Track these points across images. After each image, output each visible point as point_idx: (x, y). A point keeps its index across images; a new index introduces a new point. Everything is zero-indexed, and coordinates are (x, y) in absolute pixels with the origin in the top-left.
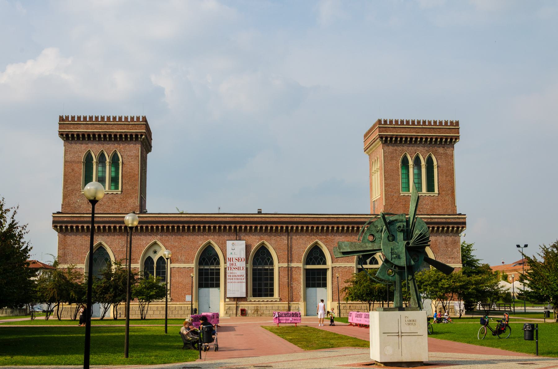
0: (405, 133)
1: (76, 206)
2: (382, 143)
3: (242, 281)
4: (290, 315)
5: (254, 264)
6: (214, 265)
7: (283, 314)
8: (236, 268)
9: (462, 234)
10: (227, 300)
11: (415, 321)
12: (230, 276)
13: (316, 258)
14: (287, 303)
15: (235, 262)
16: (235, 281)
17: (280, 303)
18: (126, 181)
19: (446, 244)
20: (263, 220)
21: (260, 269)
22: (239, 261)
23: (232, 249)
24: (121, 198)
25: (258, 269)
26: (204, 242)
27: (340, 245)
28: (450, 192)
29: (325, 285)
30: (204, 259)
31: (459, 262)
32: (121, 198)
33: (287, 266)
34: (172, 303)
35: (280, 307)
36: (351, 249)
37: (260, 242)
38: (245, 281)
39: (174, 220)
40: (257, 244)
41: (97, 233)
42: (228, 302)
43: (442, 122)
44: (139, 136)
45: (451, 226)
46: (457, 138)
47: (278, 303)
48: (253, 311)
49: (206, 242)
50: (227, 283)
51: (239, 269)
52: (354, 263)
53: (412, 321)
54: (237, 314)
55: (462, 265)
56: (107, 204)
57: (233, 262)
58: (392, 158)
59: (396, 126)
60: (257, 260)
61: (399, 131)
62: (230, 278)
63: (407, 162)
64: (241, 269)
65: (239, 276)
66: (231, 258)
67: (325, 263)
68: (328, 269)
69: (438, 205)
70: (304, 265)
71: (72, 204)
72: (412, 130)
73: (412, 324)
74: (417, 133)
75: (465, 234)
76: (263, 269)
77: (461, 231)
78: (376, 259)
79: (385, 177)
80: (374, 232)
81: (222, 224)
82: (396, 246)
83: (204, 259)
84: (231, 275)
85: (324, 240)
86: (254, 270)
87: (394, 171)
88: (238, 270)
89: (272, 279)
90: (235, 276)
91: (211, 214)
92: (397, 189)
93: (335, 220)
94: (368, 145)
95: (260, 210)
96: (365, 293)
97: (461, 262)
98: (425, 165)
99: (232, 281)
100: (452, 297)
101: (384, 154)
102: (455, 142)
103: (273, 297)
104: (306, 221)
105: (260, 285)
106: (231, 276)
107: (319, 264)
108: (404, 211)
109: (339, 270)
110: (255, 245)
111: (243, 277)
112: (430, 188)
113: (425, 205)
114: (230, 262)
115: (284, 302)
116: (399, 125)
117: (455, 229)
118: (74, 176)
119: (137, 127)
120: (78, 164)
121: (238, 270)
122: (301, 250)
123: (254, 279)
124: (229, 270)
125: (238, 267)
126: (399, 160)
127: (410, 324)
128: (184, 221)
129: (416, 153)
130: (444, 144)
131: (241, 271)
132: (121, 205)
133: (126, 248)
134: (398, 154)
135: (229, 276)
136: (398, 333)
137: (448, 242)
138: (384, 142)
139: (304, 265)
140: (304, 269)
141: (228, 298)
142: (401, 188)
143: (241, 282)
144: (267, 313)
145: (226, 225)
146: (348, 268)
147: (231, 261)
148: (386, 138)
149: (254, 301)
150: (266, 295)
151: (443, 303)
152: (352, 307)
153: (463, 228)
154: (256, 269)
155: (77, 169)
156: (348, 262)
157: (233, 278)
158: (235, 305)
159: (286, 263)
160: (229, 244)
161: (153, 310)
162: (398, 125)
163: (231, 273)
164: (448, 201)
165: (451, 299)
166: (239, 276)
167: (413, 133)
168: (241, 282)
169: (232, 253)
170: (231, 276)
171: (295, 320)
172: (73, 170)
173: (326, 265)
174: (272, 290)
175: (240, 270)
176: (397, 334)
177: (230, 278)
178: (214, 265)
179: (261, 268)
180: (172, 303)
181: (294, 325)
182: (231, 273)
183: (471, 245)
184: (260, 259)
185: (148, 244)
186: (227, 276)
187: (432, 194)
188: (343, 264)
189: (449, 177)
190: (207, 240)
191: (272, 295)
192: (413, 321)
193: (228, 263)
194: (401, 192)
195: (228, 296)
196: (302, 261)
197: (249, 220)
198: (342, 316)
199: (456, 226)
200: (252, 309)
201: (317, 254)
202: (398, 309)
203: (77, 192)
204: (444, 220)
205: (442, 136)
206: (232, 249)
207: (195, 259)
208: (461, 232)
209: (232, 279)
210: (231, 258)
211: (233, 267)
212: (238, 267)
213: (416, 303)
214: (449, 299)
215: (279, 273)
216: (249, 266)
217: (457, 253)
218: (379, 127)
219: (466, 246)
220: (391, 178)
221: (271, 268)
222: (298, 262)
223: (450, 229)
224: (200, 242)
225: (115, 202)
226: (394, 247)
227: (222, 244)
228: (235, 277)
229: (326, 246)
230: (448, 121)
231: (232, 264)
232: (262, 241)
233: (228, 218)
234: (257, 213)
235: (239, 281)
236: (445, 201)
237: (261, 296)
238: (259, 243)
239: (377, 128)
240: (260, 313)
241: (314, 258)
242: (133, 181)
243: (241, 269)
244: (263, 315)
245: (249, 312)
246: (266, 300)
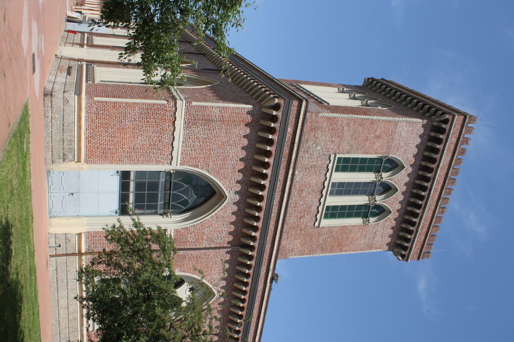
1: (310, 143)
18: (334, 233)
24: (306, 226)
32: (306, 226)
41: (248, 189)
44: (404, 253)
56: (301, 203)
71: (314, 136)
118: (367, 139)
119: (418, 248)
120: (385, 147)
132: (293, 229)
133: (207, 246)
155: (378, 144)
172: (378, 137)
203: (335, 145)
225: (301, 218)
242: (333, 244)
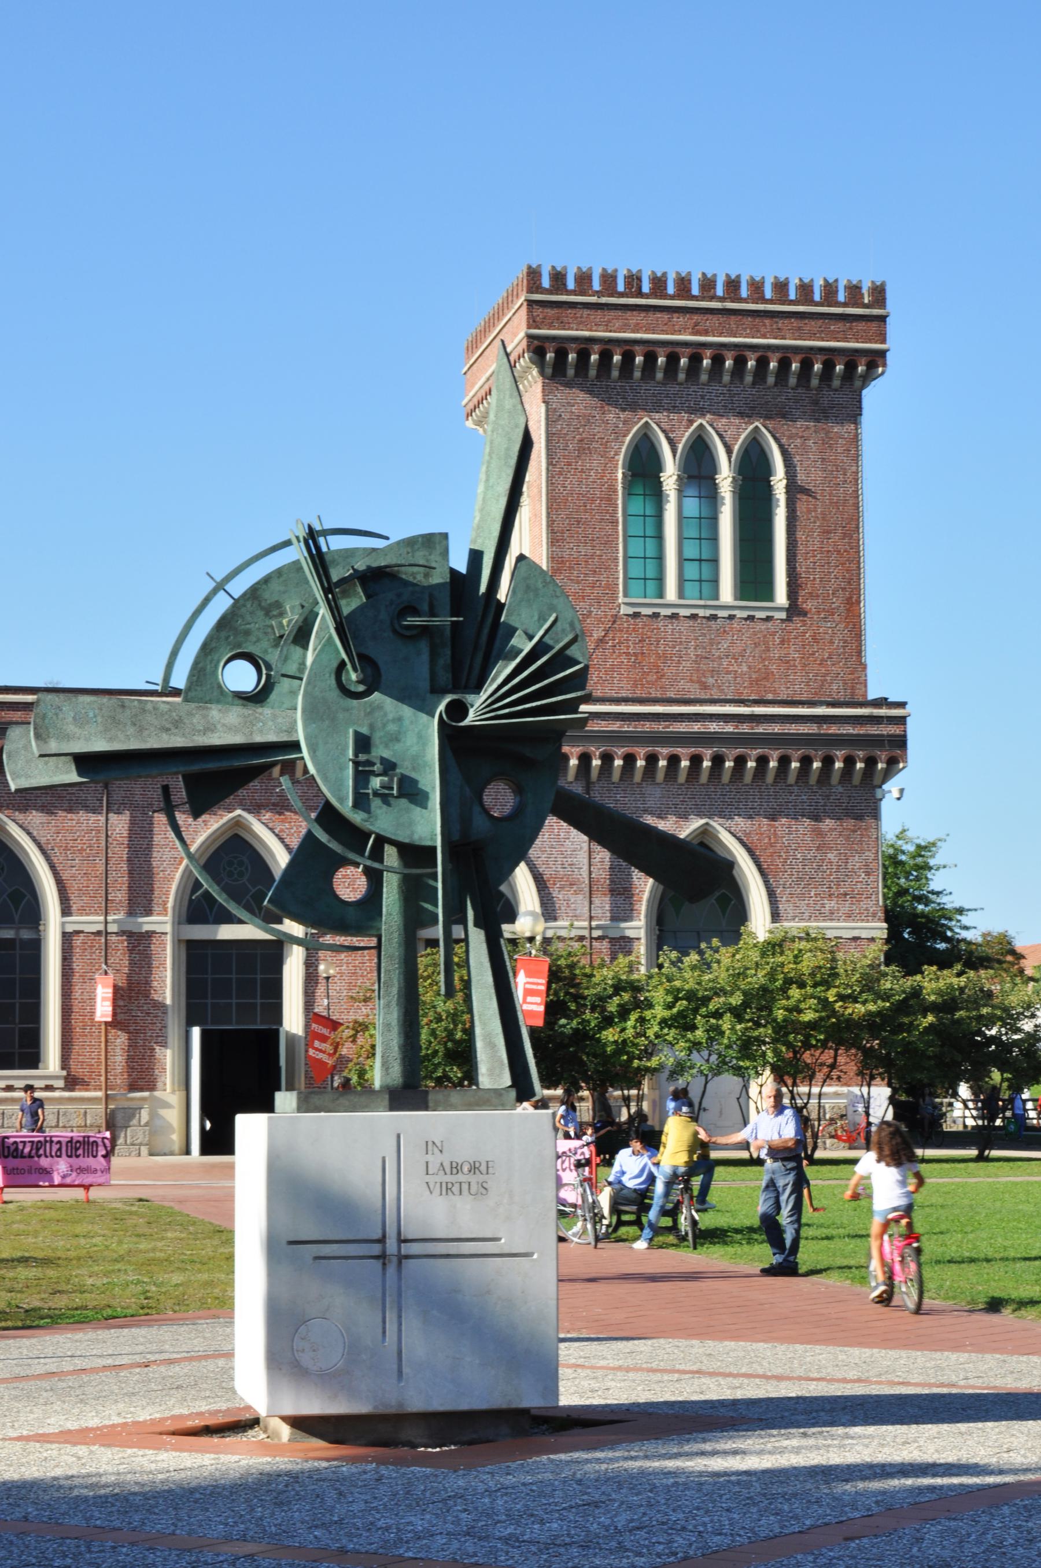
0: (647, 331)
2: (542, 373)
4: (60, 1149)
7: (24, 1143)
9: (892, 787)
11: (483, 1168)
14: (100, 1094)
17: (67, 1094)
27: (50, 715)
28: (837, 602)
31: (874, 915)
33: (101, 927)
35: (65, 1114)
36: (111, 740)
43: (812, 286)
45: (840, 753)
46: (876, 359)
53: (466, 1169)
55: (885, 925)
58: (584, 449)
59: (604, 300)
63: (657, 465)
69: (785, 661)
70: (179, 923)
72: (679, 320)
73: (465, 1187)
75: (902, 791)
77: (888, 774)
80: (258, 640)
82: (384, 725)
87: (593, 501)
92: (608, 586)
94: (481, 387)
96: (441, 1049)
97: (881, 915)
98: (730, 479)
100: (833, 1066)
101: (547, 425)
102: (868, 377)
108: (635, 686)
113: (727, 656)
116: (622, 295)
117: (859, 765)
126: (616, 455)
127: (456, 1189)
129: (691, 422)
130: (819, 388)
134: (610, 427)
136: (378, 1241)
138: (549, 371)
139: (178, 922)
140: (179, 941)
142: (621, 580)
148: (561, 354)
151: (791, 1092)
153: (892, 762)
162: (614, 293)
164: (832, 642)
165: (828, 1077)
167: (679, 332)
171: (81, 1170)
176: (376, 1249)
181: (79, 1194)
183: (934, 844)
187: (759, 609)
189: (835, 537)
191: (32, 1058)
192: (474, 1168)
194: (620, 601)
196: (170, 905)
199: (861, 754)
201: (241, 874)
202: (387, 1096)
205: (811, 349)
208: (884, 782)
213: (502, 1064)
214: (820, 1076)
217: (868, 874)
219: (910, 848)
220: (577, 532)
221: (26, 935)
223: (838, 765)
226: (372, 727)
230: (836, 281)
236: (815, 640)
239: (522, 304)
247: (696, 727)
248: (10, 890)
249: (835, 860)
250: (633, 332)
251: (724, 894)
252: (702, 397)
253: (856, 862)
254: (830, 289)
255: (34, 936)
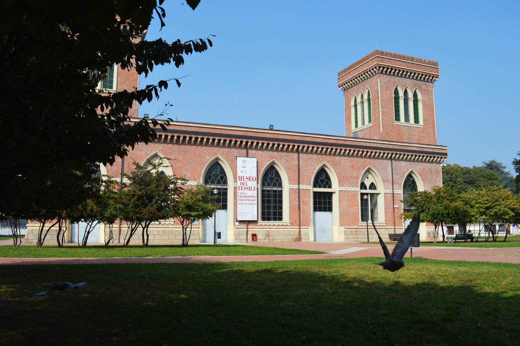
0: (399, 66)
3: (253, 202)
5: (263, 184)
6: (221, 184)
8: (248, 188)
10: (237, 224)
12: (241, 197)
13: (322, 181)
14: (298, 227)
15: (246, 181)
16: (246, 202)
17: (291, 227)
19: (431, 173)
20: (276, 136)
21: (269, 191)
22: (250, 181)
23: (243, 167)
25: (267, 190)
26: (212, 157)
28: (431, 125)
29: (330, 209)
30: (210, 177)
34: (176, 226)
37: (271, 161)
38: (256, 202)
39: (180, 129)
40: (268, 163)
42: (237, 226)
47: (289, 227)
48: (264, 236)
49: (214, 157)
50: (238, 205)
51: (250, 189)
52: (358, 187)
54: (247, 239)
57: (244, 181)
60: (266, 180)
61: (393, 63)
62: (240, 198)
64: (253, 189)
65: (250, 197)
66: (241, 176)
67: (330, 187)
68: (334, 192)
72: (404, 64)
74: (407, 67)
76: (272, 190)
78: (375, 185)
79: (382, 106)
81: (233, 138)
83: (210, 177)
84: (242, 195)
85: (331, 163)
86: (263, 191)
87: (389, 100)
88: (249, 190)
89: (281, 202)
90: (246, 197)
91: (221, 125)
93: (342, 142)
95: (272, 126)
99: (242, 202)
103: (282, 221)
104: (317, 141)
105: (269, 208)
106: (242, 197)
107: (325, 187)
109: (346, 194)
110: (267, 164)
111: (255, 199)
112: (417, 121)
114: (240, 181)
115: (295, 226)
121: (249, 190)
122: (311, 172)
123: (263, 201)
124: (239, 190)
125: (249, 187)
128: (191, 131)
129: (405, 86)
131: (252, 191)
134: (391, 85)
135: (240, 196)
137: (433, 171)
141: (237, 221)
143: (252, 204)
144: (279, 238)
145: (237, 139)
146: (353, 192)
147: (241, 180)
149: (265, 225)
150: (275, 219)
152: (357, 232)
153: (445, 158)
154: (265, 190)
156: (353, 186)
157: (244, 199)
158: (246, 229)
159: (296, 185)
160: (240, 160)
161: (154, 234)
163: (242, 193)
166: (250, 197)
168: (252, 204)
169: (242, 171)
170: (242, 197)
173: (331, 188)
174: (281, 214)
175: (251, 190)
177: (240, 198)
178: (221, 184)
179: (270, 189)
180: (176, 226)
182: (242, 193)
184: (269, 180)
185: (148, 155)
186: (238, 197)
188: (348, 188)
189: (430, 112)
190: (215, 155)
193: (239, 182)
195: (238, 220)
197: (261, 136)
198: (370, 241)
199: (440, 156)
200: (263, 234)
204: (431, 150)
206: (243, 167)
207: (202, 176)
209: (243, 200)
210: (241, 176)
211: (244, 186)
212: (249, 187)
215: (290, 195)
216: (259, 187)
218: (377, 56)
221: (279, 189)
222: (307, 185)
224: (208, 157)
227: (232, 160)
228: (246, 198)
229: (333, 168)
231: (243, 184)
232: (273, 160)
233: (239, 132)
234: (269, 128)
235: (251, 202)
237: (270, 221)
238: (270, 162)
240: (272, 239)
241: (321, 180)
243: (253, 189)
244: (275, 241)
245: (259, 237)
246: (276, 224)
247: (412, 149)
248: (276, 179)
249: (434, 178)
250: (396, 65)
251: (407, 185)
252: (407, 81)
253: (438, 179)
254: (429, 62)
255: (281, 190)
